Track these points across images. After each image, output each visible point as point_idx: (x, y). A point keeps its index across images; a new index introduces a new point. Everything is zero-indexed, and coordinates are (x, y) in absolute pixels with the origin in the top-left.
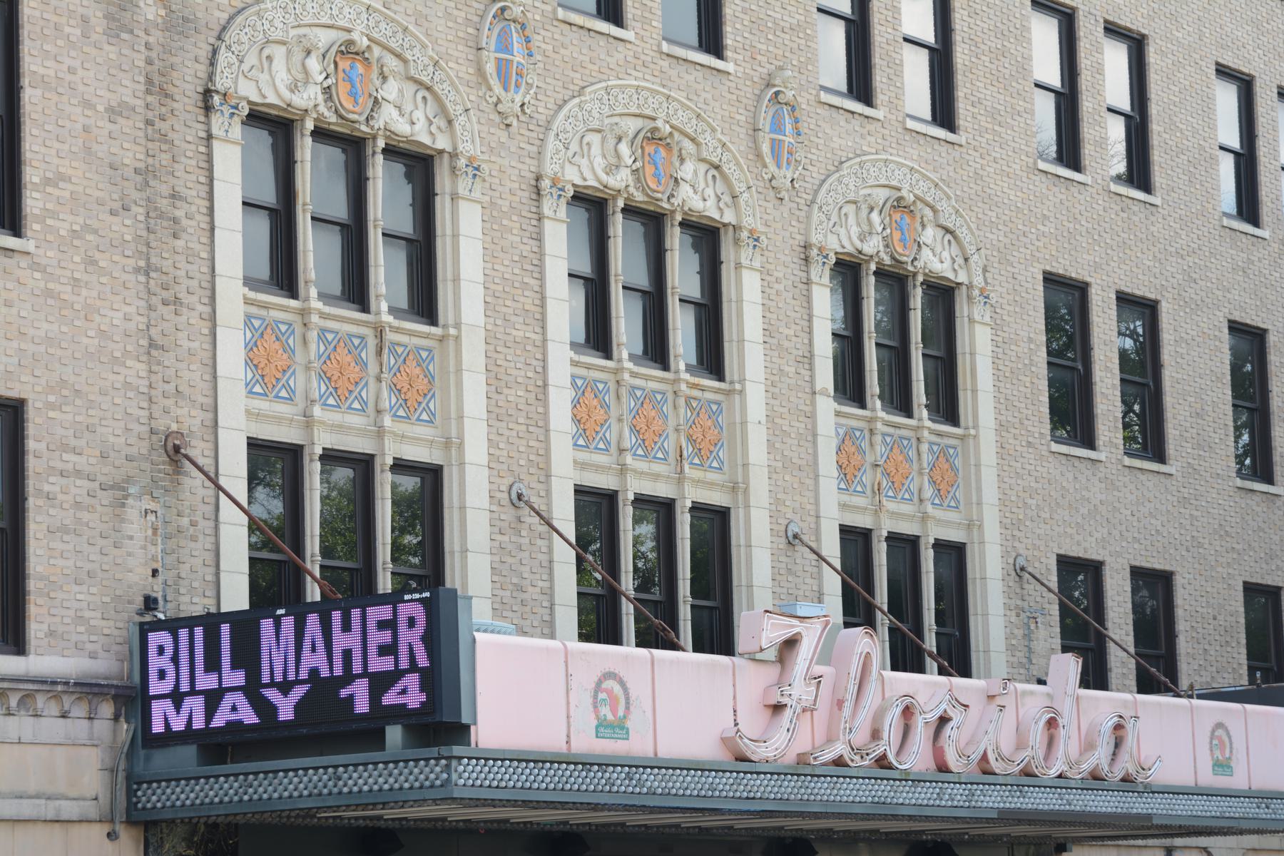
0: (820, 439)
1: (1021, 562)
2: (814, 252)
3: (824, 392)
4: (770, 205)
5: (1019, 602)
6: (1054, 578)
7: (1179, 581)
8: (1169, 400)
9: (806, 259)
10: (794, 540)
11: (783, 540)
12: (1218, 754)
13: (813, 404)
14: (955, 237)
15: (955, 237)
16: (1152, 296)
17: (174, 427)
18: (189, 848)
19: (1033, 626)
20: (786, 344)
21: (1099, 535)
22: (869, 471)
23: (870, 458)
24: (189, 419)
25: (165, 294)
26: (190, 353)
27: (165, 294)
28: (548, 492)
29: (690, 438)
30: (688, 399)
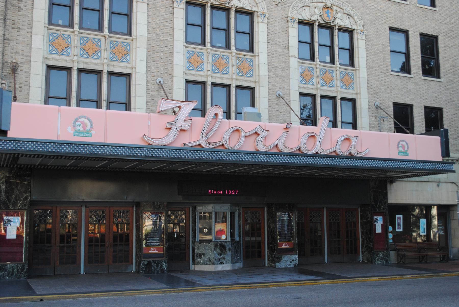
0: (290, 69)
1: (376, 104)
2: (289, 19)
3: (293, 56)
4: (273, 6)
5: (377, 115)
6: (392, 109)
7: (444, 111)
8: (441, 62)
9: (287, 21)
10: (279, 97)
11: (275, 96)
12: (401, 149)
13: (289, 59)
14: (352, 17)
15: (352, 17)
16: (435, 35)
17: (14, 61)
18: (10, 174)
19: (382, 121)
20: (278, 43)
21: (411, 97)
22: (315, 78)
23: (315, 75)
24: (19, 59)
25: (13, 26)
26: (23, 42)
27: (13, 26)
28: (172, 81)
29: (238, 68)
30: (237, 58)
